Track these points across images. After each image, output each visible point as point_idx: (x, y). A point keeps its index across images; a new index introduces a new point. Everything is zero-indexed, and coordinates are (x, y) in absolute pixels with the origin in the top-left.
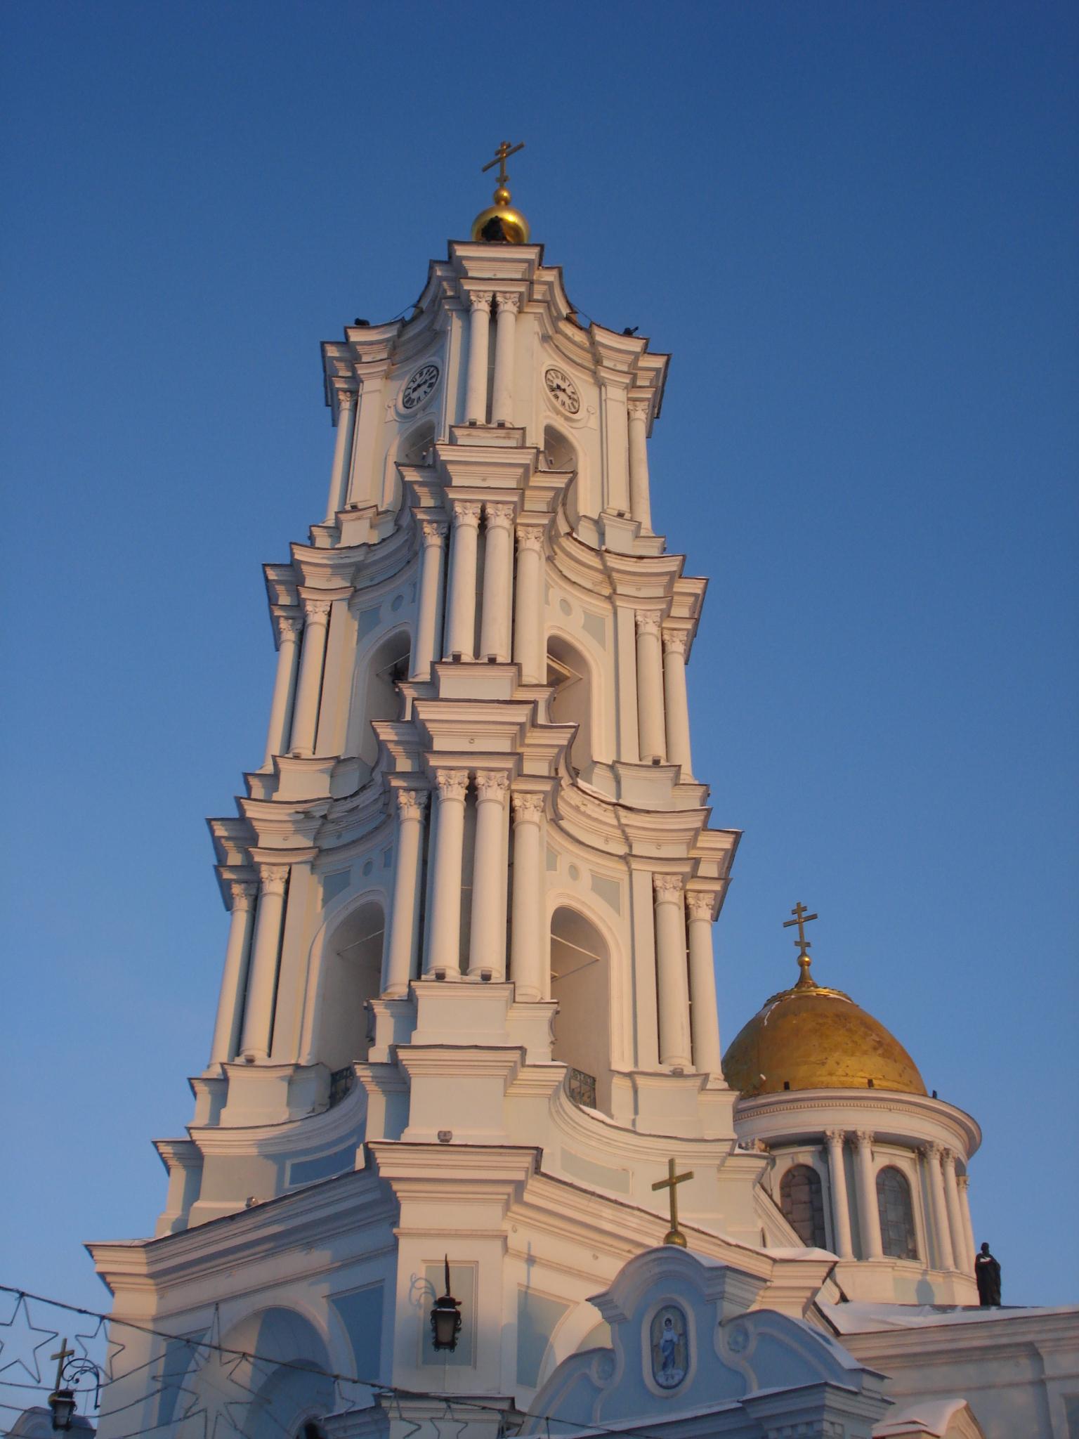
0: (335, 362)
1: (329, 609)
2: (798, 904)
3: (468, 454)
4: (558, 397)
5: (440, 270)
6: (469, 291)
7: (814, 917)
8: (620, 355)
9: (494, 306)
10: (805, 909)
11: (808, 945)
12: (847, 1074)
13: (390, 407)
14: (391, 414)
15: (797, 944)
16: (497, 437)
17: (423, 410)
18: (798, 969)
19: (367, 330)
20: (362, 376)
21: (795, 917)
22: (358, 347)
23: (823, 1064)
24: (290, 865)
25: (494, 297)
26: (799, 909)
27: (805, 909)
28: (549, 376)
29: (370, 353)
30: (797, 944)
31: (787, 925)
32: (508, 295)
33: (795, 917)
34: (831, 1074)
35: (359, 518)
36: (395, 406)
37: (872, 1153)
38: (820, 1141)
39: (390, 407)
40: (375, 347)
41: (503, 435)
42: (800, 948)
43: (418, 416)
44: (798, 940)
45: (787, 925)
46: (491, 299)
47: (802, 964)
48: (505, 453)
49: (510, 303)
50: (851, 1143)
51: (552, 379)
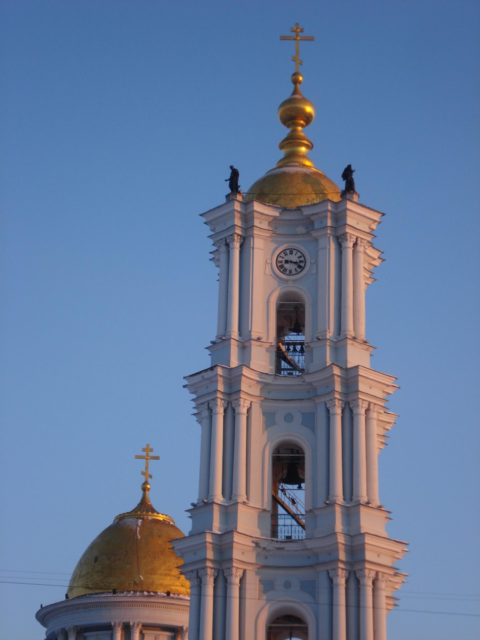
0: (235, 212)
1: (249, 406)
2: (148, 445)
5: (330, 206)
6: (347, 233)
7: (157, 458)
8: (369, 258)
10: (151, 450)
11: (151, 477)
13: (268, 264)
14: (268, 271)
15: (143, 473)
16: (363, 349)
17: (293, 281)
18: (141, 492)
19: (263, 205)
20: (254, 235)
21: (144, 454)
22: (255, 213)
26: (148, 449)
27: (151, 450)
29: (259, 219)
31: (138, 457)
32: (363, 241)
33: (144, 454)
35: (260, 346)
36: (271, 263)
39: (268, 264)
40: (264, 217)
41: (365, 348)
42: (144, 476)
43: (289, 283)
44: (144, 471)
45: (138, 457)
47: (144, 489)
48: (384, 377)
49: (363, 246)
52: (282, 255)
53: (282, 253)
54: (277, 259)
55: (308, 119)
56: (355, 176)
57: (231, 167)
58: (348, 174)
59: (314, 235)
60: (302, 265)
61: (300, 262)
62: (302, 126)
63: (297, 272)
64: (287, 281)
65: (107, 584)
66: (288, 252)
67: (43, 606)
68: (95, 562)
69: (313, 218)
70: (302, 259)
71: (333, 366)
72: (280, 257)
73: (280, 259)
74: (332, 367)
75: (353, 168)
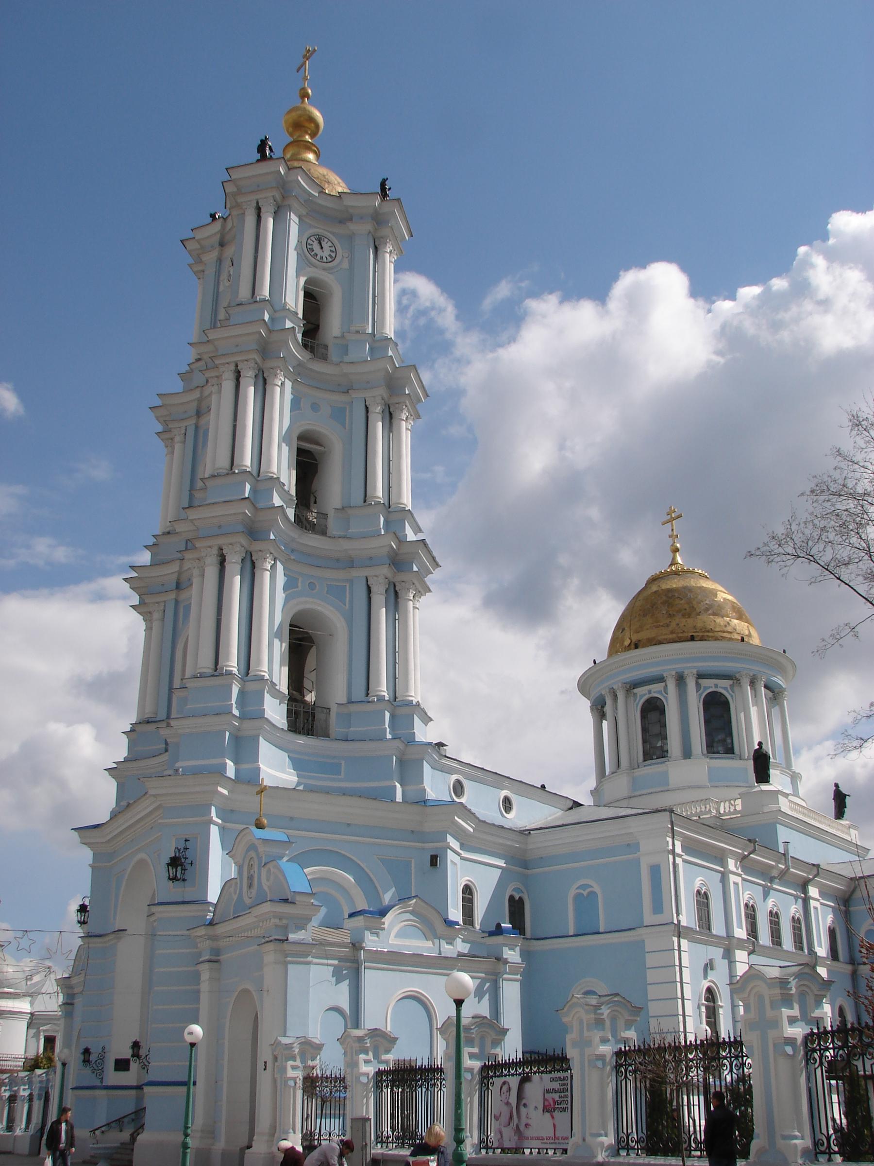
4: (317, 255)
9: (259, 209)
12: (684, 631)
15: (670, 536)
23: (668, 626)
24: (165, 602)
25: (257, 203)
28: (309, 241)
30: (670, 536)
34: (672, 632)
37: (698, 685)
38: (661, 679)
44: (671, 533)
46: (255, 205)
50: (680, 679)
51: (311, 242)
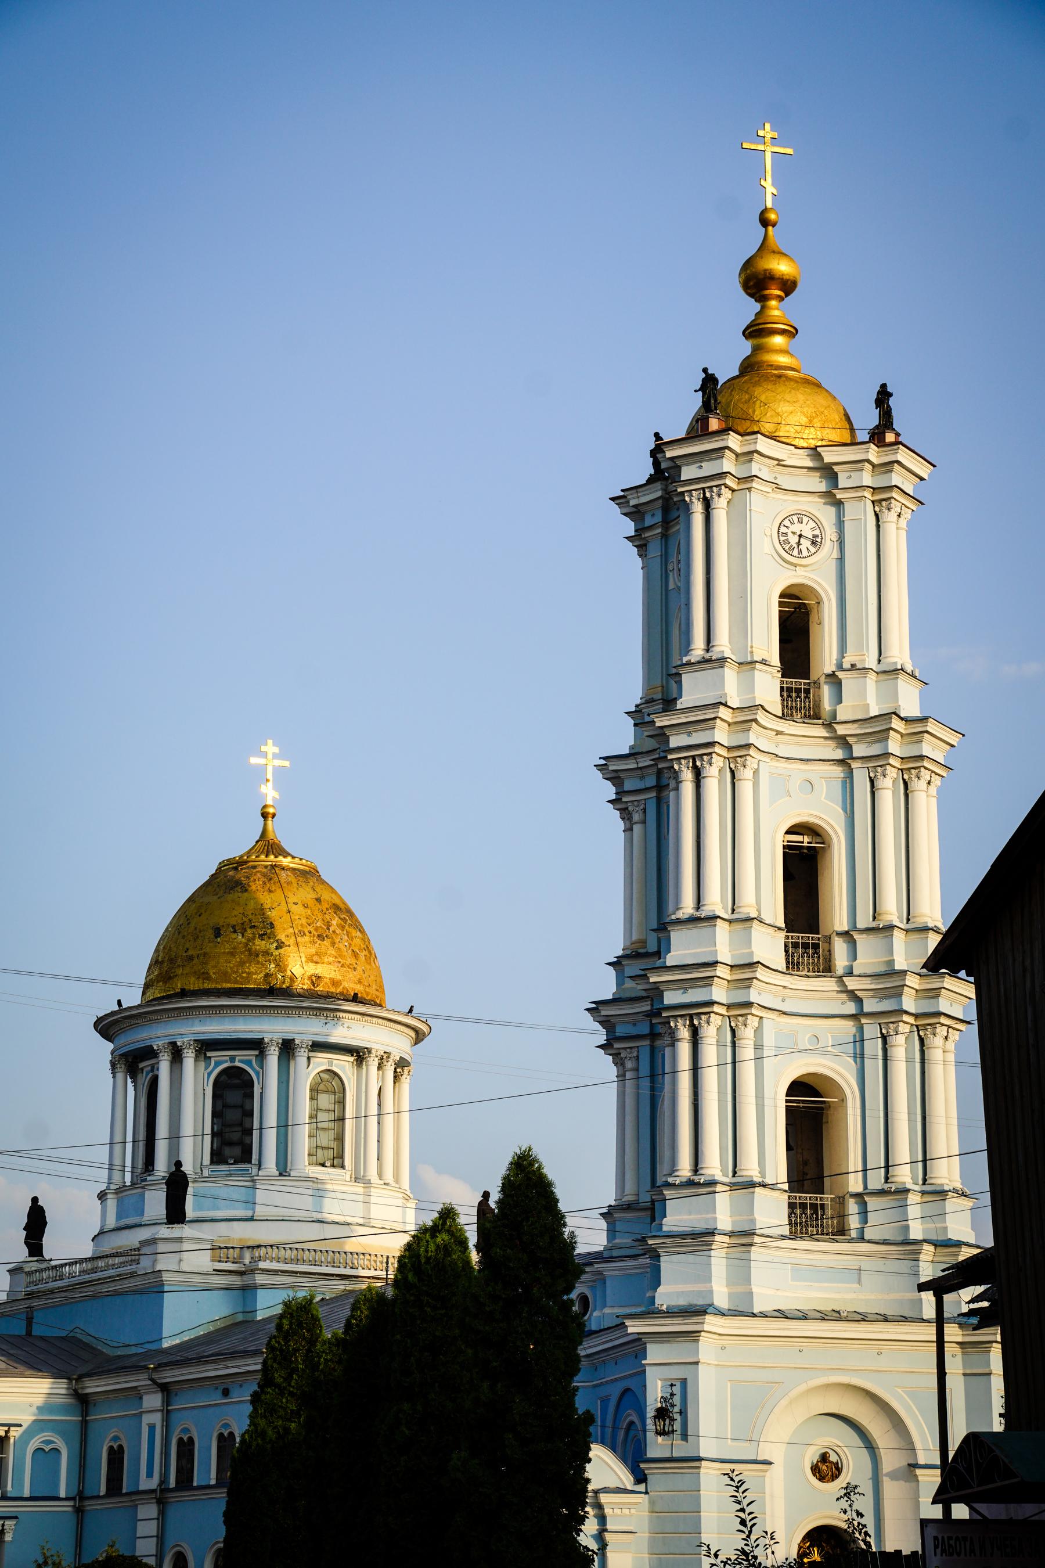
3: (939, 730)
52: (787, 523)
53: (787, 520)
54: (779, 529)
55: (788, 287)
56: (892, 401)
57: (705, 370)
58: (883, 396)
59: (838, 497)
60: (819, 540)
61: (814, 536)
62: (781, 299)
63: (810, 554)
64: (795, 565)
65: (244, 975)
66: (795, 518)
67: (124, 1006)
68: (216, 937)
69: (836, 468)
70: (817, 532)
71: (893, 716)
72: (784, 526)
73: (783, 529)
74: (891, 718)
75: (889, 389)
